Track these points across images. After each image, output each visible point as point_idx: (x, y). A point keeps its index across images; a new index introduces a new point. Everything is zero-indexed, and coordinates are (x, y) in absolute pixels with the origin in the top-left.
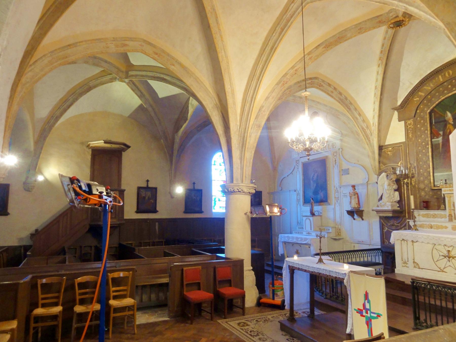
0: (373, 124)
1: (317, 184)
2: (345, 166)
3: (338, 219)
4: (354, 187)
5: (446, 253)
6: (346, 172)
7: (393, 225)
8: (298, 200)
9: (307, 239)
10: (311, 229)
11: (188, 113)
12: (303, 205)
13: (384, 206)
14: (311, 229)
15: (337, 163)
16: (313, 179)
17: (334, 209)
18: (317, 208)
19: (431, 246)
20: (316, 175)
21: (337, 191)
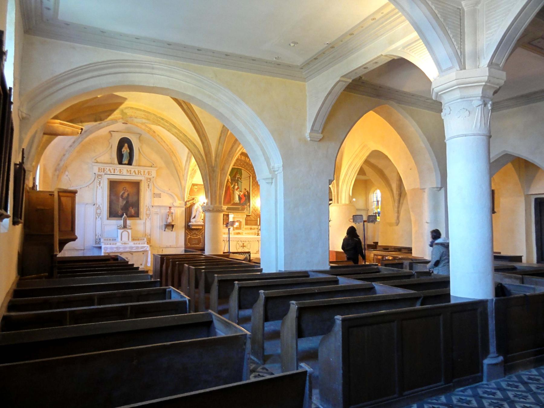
0: (193, 169)
1: (127, 202)
2: (157, 191)
3: (148, 231)
4: (170, 208)
5: (242, 245)
6: (159, 196)
7: (195, 234)
8: (98, 215)
9: (144, 247)
10: (128, 240)
11: (109, 116)
12: (107, 219)
13: (198, 222)
14: (128, 240)
15: (150, 188)
16: (122, 196)
17: (145, 224)
18: (129, 222)
19: (235, 243)
20: (126, 194)
21: (148, 209)
